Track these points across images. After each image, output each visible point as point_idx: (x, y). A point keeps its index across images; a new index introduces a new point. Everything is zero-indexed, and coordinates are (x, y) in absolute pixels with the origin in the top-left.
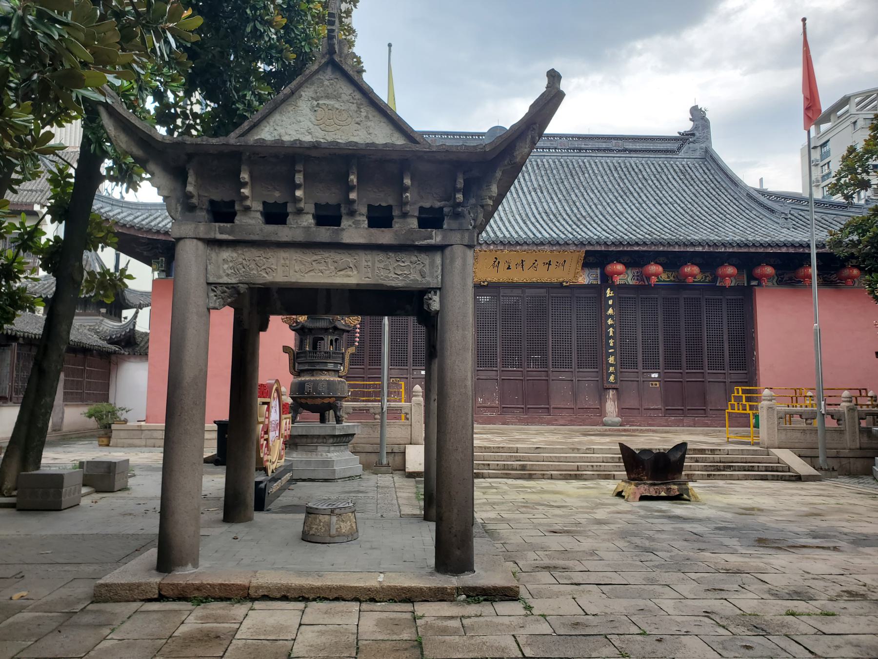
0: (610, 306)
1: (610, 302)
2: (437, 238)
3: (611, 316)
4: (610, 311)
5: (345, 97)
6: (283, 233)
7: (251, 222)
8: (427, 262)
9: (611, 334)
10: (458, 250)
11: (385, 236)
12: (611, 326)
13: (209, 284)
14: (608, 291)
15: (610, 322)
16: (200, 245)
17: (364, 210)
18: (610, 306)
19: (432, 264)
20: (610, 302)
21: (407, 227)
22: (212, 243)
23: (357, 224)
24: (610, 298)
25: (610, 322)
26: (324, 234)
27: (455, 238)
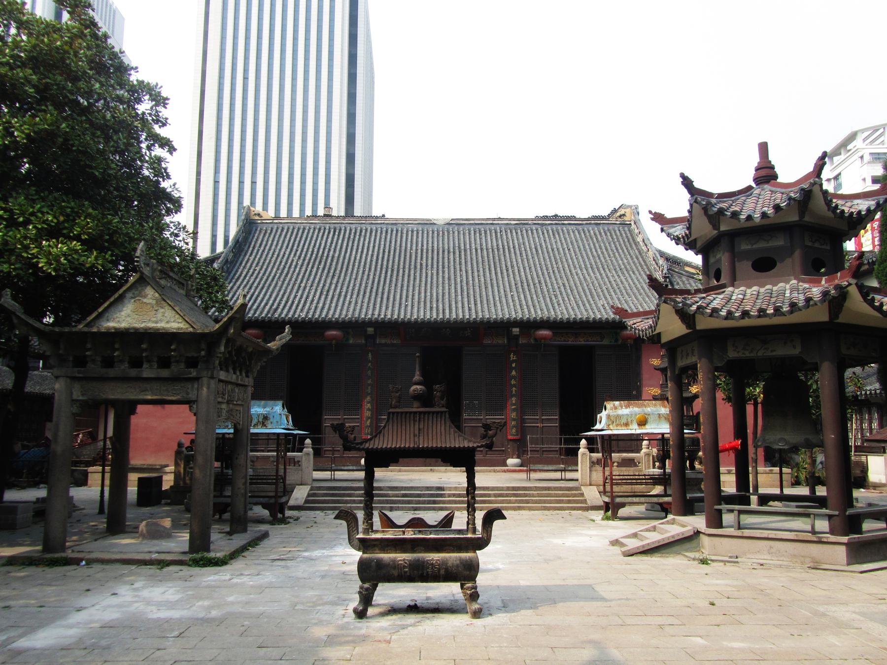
0: (514, 368)
1: (514, 365)
2: (194, 373)
3: (514, 377)
4: (514, 373)
5: (149, 296)
6: (112, 372)
7: (94, 368)
8: (190, 386)
10: (205, 380)
11: (165, 373)
12: (514, 385)
13: (73, 400)
15: (513, 382)
16: (68, 380)
17: (155, 359)
18: (514, 368)
19: (193, 387)
20: (514, 365)
21: (177, 369)
22: (74, 379)
23: (151, 367)
24: (514, 361)
25: (513, 382)
26: (133, 372)
27: (205, 373)
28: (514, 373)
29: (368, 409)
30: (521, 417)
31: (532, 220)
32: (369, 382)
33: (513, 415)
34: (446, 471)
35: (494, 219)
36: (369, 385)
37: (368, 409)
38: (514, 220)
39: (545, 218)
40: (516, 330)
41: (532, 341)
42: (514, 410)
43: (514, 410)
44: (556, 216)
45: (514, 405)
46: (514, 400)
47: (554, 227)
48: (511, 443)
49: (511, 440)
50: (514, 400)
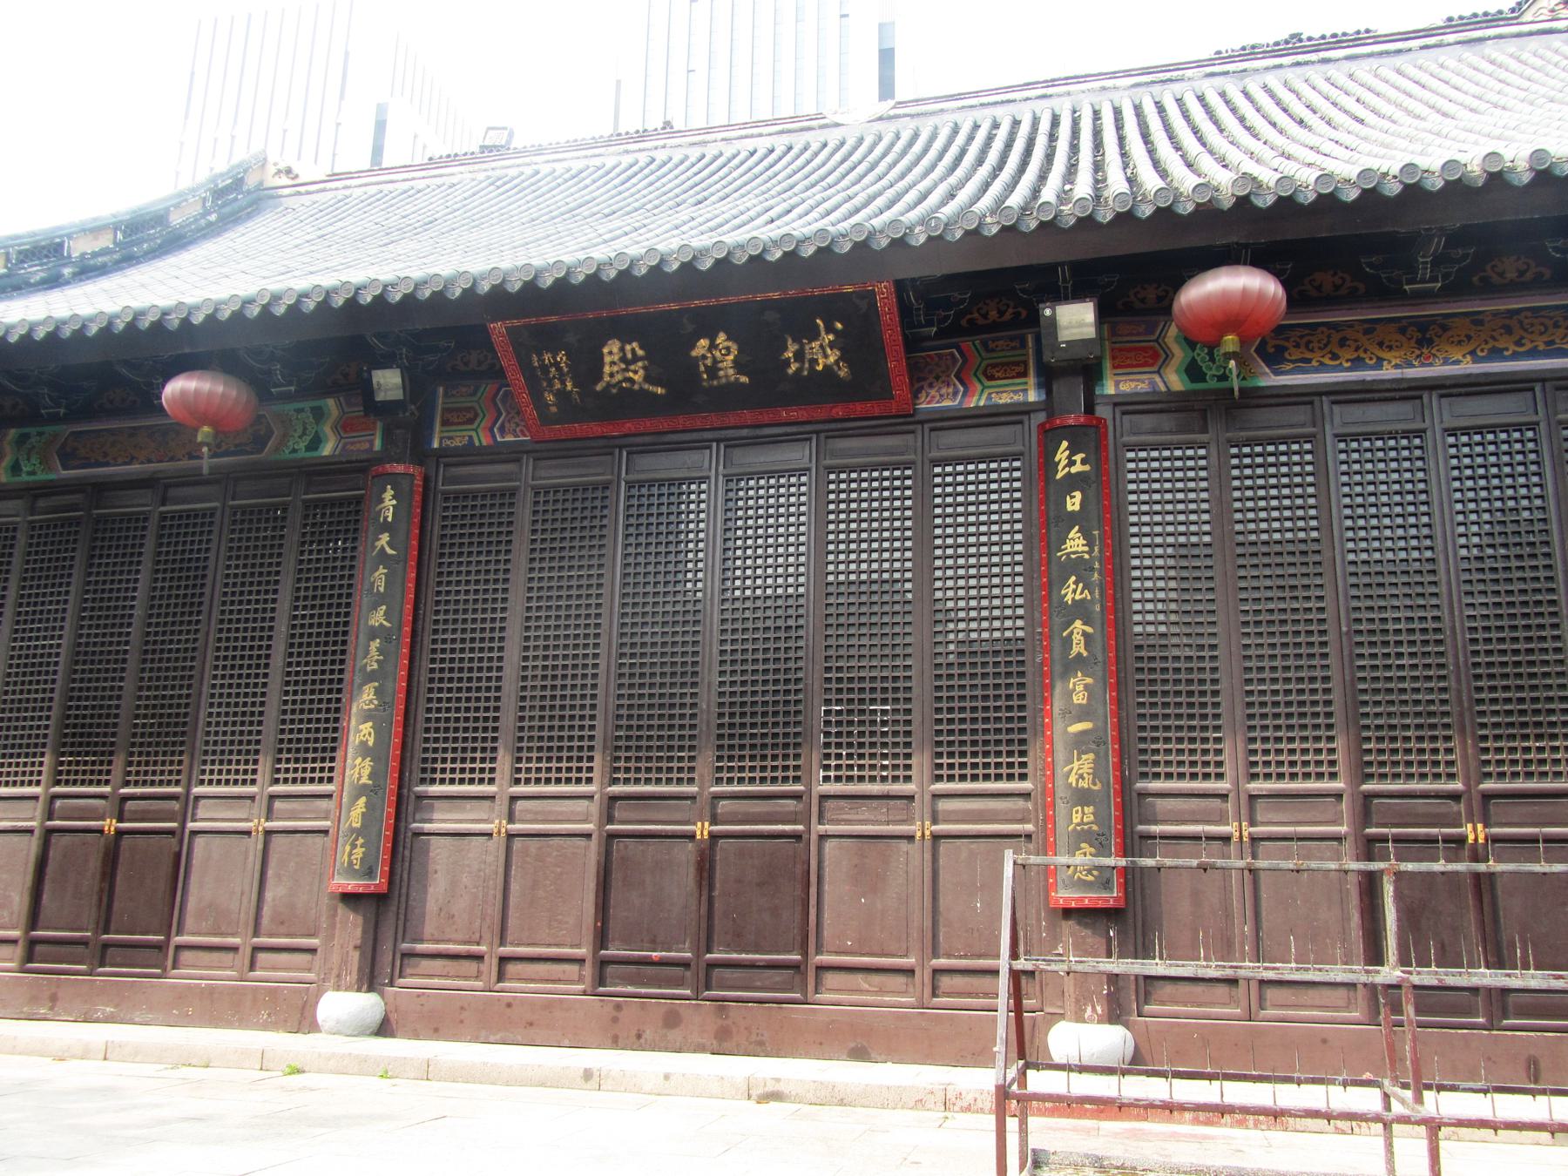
0: (1073, 519)
1: (1074, 503)
4: (1075, 543)
9: (1078, 648)
12: (1080, 610)
14: (1062, 455)
15: (1072, 592)
24: (1073, 482)
25: (1072, 592)
28: (1075, 543)
29: (365, 751)
30: (1124, 785)
31: (1199, 64)
32: (378, 618)
33: (1079, 771)
34: (668, 1085)
35: (1052, 83)
36: (373, 633)
37: (365, 751)
38: (1127, 73)
39: (1250, 52)
40: (1076, 320)
41: (1175, 380)
42: (1080, 743)
43: (1080, 743)
44: (1297, 37)
45: (1083, 713)
46: (1078, 688)
47: (1290, 74)
48: (1068, 926)
49: (1067, 913)
50: (1078, 688)
